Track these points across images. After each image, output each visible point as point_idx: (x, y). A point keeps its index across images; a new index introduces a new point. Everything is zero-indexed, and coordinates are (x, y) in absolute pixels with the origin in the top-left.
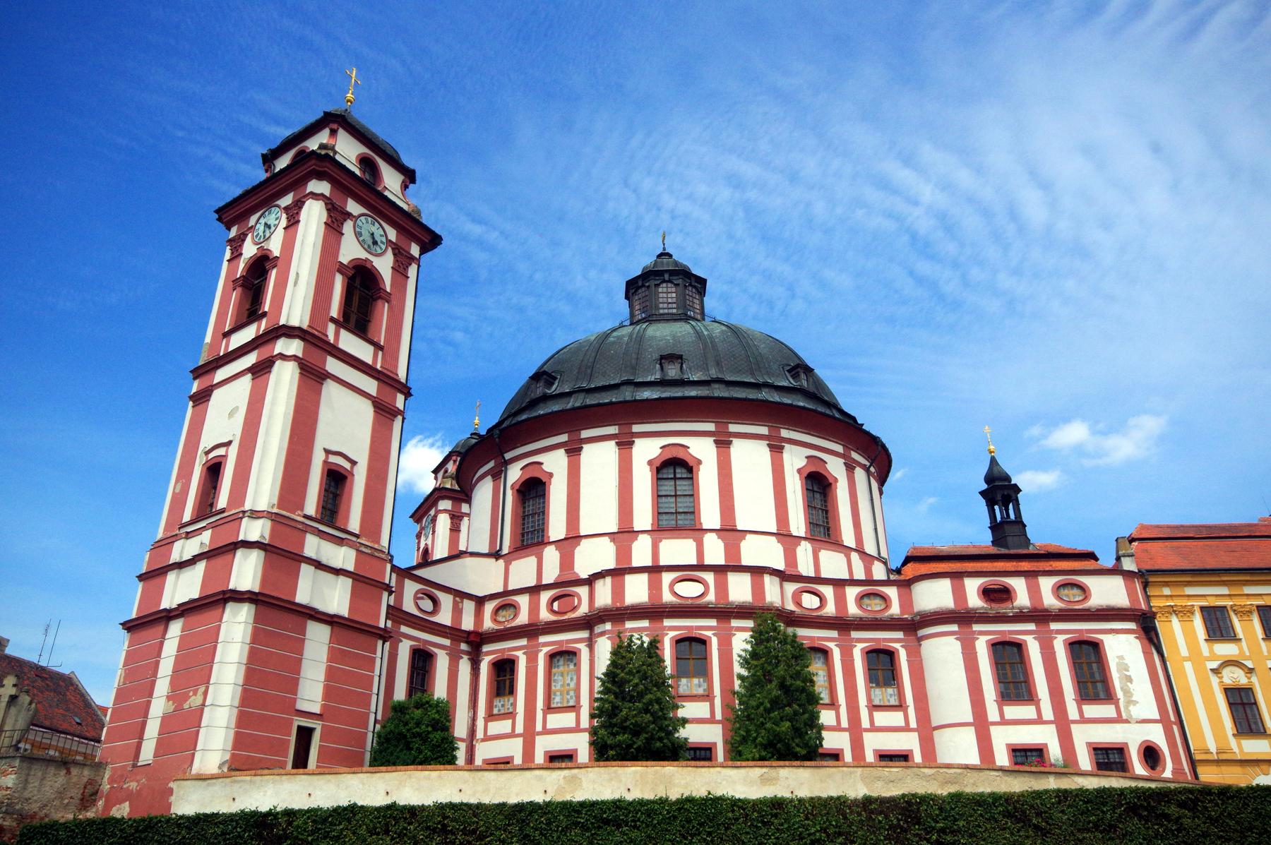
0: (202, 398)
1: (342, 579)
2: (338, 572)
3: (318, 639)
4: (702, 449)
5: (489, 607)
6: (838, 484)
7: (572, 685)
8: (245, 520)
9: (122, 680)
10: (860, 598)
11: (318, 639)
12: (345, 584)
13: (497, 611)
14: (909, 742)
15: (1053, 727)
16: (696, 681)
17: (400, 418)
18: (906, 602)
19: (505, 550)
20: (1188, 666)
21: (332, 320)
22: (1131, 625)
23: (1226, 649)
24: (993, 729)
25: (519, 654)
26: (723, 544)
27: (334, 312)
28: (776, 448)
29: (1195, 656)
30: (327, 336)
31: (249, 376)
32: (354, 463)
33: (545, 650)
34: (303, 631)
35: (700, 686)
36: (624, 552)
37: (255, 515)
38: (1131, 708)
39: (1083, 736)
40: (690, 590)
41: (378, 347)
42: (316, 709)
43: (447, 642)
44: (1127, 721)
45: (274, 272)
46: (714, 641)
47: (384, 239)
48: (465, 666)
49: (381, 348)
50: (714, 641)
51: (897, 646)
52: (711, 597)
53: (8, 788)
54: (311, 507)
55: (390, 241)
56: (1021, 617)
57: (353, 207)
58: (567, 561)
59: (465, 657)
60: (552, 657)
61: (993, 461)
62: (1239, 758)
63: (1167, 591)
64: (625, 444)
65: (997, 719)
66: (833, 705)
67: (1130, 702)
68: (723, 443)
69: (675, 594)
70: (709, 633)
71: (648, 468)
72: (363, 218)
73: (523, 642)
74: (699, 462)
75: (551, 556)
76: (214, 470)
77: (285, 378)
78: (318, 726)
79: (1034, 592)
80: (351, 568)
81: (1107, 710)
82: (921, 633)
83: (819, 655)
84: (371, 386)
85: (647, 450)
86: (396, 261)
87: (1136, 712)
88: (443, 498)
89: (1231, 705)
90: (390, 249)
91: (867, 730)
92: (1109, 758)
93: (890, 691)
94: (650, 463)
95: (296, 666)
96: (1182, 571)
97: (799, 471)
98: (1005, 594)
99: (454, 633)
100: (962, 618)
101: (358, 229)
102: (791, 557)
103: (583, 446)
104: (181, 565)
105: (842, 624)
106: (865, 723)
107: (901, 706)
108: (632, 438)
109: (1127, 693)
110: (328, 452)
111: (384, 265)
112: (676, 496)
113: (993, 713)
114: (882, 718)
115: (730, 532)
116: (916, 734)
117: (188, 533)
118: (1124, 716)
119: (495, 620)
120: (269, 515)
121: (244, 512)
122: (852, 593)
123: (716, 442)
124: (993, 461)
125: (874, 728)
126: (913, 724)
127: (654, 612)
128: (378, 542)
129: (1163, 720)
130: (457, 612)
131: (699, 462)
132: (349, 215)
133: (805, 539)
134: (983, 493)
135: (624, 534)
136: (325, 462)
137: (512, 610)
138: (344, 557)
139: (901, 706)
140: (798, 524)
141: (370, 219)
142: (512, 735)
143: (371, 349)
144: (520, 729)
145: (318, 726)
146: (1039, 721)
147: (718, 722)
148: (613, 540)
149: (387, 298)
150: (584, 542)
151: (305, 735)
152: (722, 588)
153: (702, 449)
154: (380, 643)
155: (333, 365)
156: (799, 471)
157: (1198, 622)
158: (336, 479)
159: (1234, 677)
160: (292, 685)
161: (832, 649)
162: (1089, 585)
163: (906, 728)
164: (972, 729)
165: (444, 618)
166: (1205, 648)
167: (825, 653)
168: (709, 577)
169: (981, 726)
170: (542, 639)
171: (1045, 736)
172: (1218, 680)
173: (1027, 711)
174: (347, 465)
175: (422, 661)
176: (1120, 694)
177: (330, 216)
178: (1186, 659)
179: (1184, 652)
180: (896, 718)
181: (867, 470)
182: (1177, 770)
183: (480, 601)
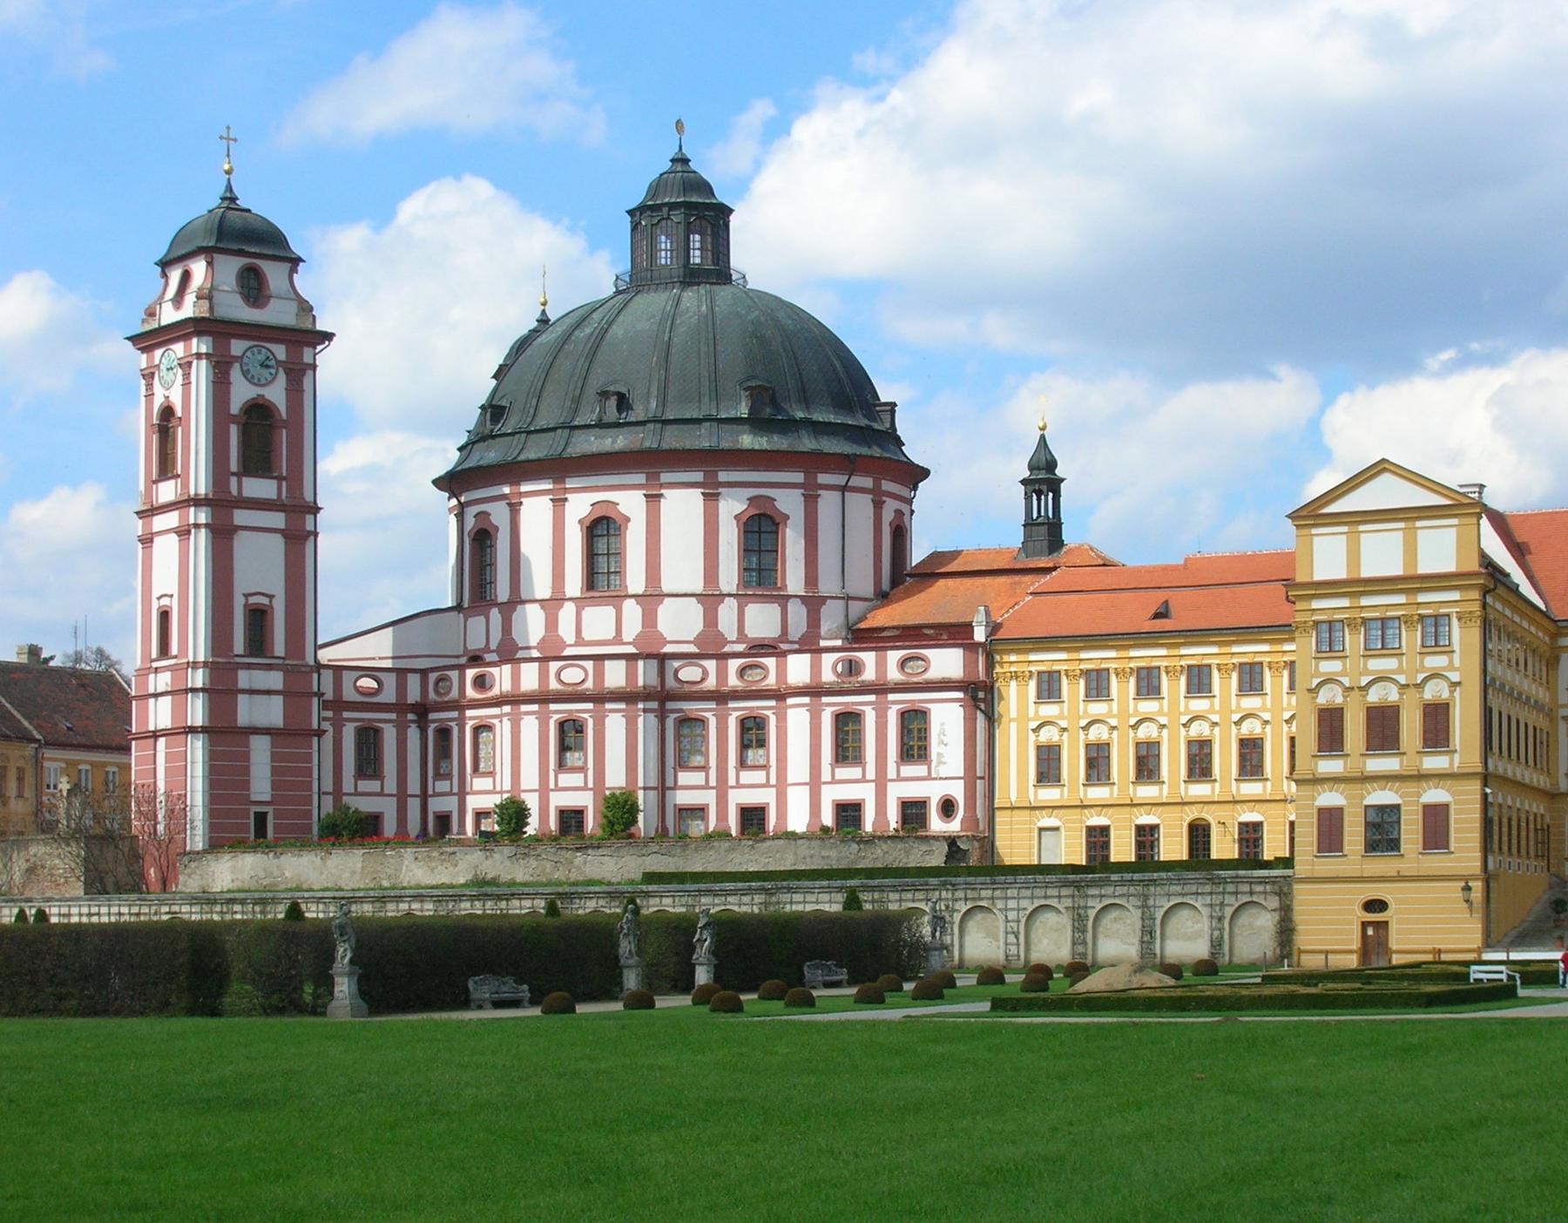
0: (147, 540)
1: (274, 697)
2: (268, 692)
3: (260, 749)
4: (630, 503)
5: (433, 677)
6: (788, 522)
8: (190, 670)
10: (742, 672)
11: (260, 749)
12: (277, 703)
13: (439, 680)
14: (766, 797)
15: (873, 784)
16: (577, 755)
17: (312, 538)
18: (782, 672)
19: (466, 605)
20: (1013, 726)
21: (234, 474)
22: (960, 695)
23: (1049, 710)
24: (824, 787)
25: (453, 724)
26: (640, 610)
27: (234, 467)
28: (711, 498)
29: (1023, 718)
30: (230, 492)
31: (174, 538)
32: (271, 597)
34: (247, 745)
35: (580, 759)
38: (941, 768)
39: (897, 792)
40: (572, 675)
41: (280, 479)
42: (267, 798)
43: (393, 716)
44: (935, 779)
45: (180, 429)
46: (590, 722)
47: (273, 363)
48: (413, 734)
49: (284, 478)
50: (590, 722)
51: (768, 713)
52: (589, 684)
54: (239, 646)
55: (280, 362)
56: (865, 689)
57: (237, 347)
59: (413, 726)
61: (1043, 438)
62: (1033, 805)
63: (1013, 658)
64: (559, 503)
65: (829, 779)
66: (704, 768)
67: (940, 763)
69: (560, 681)
70: (585, 716)
71: (579, 527)
72: (248, 354)
73: (455, 714)
74: (628, 520)
75: (495, 614)
76: (165, 616)
77: (201, 539)
78: (269, 809)
79: (881, 666)
80: (279, 686)
81: (920, 770)
82: (790, 701)
83: (699, 723)
84: (277, 520)
85: (580, 505)
86: (288, 381)
87: (943, 772)
89: (1039, 760)
90: (281, 370)
91: (732, 787)
92: (913, 812)
93: (761, 752)
94: (580, 521)
95: (246, 771)
97: (736, 517)
98: (853, 668)
99: (400, 707)
100: (815, 691)
101: (245, 368)
102: (711, 619)
103: (522, 500)
104: (156, 695)
105: (721, 697)
106: (732, 781)
107: (765, 767)
108: (565, 493)
109: (940, 755)
110: (247, 596)
111: (276, 394)
113: (826, 775)
114: (747, 777)
115: (652, 598)
116: (774, 790)
117: (156, 668)
118: (934, 775)
119: (437, 692)
120: (205, 664)
122: (734, 665)
125: (739, 786)
126: (773, 781)
127: (543, 698)
128: (304, 659)
129: (970, 778)
130: (401, 688)
131: (628, 520)
132: (236, 359)
133: (730, 595)
134: (1024, 482)
135: (553, 604)
136: (246, 605)
137: (448, 683)
138: (275, 680)
139: (765, 767)
140: (729, 577)
141: (255, 349)
142: (450, 794)
143: (275, 482)
144: (455, 790)
145: (269, 809)
146: (863, 780)
147: (591, 789)
148: (542, 608)
149: (285, 424)
151: (261, 819)
152: (599, 675)
153: (630, 503)
154: (315, 739)
155: (241, 517)
156: (736, 517)
157: (1032, 685)
158: (258, 617)
159: (1049, 735)
160: (246, 785)
161: (708, 719)
162: (930, 658)
163: (767, 785)
164: (807, 788)
165: (389, 696)
166: (1032, 706)
167: (702, 722)
168: (589, 665)
169: (815, 784)
170: (469, 713)
171: (864, 793)
172: (1035, 738)
173: (855, 772)
174: (265, 601)
175: (369, 740)
176: (934, 756)
177: (215, 374)
178: (1014, 720)
179: (1013, 714)
180: (759, 777)
181: (844, 489)
182: (970, 820)
183: (424, 673)
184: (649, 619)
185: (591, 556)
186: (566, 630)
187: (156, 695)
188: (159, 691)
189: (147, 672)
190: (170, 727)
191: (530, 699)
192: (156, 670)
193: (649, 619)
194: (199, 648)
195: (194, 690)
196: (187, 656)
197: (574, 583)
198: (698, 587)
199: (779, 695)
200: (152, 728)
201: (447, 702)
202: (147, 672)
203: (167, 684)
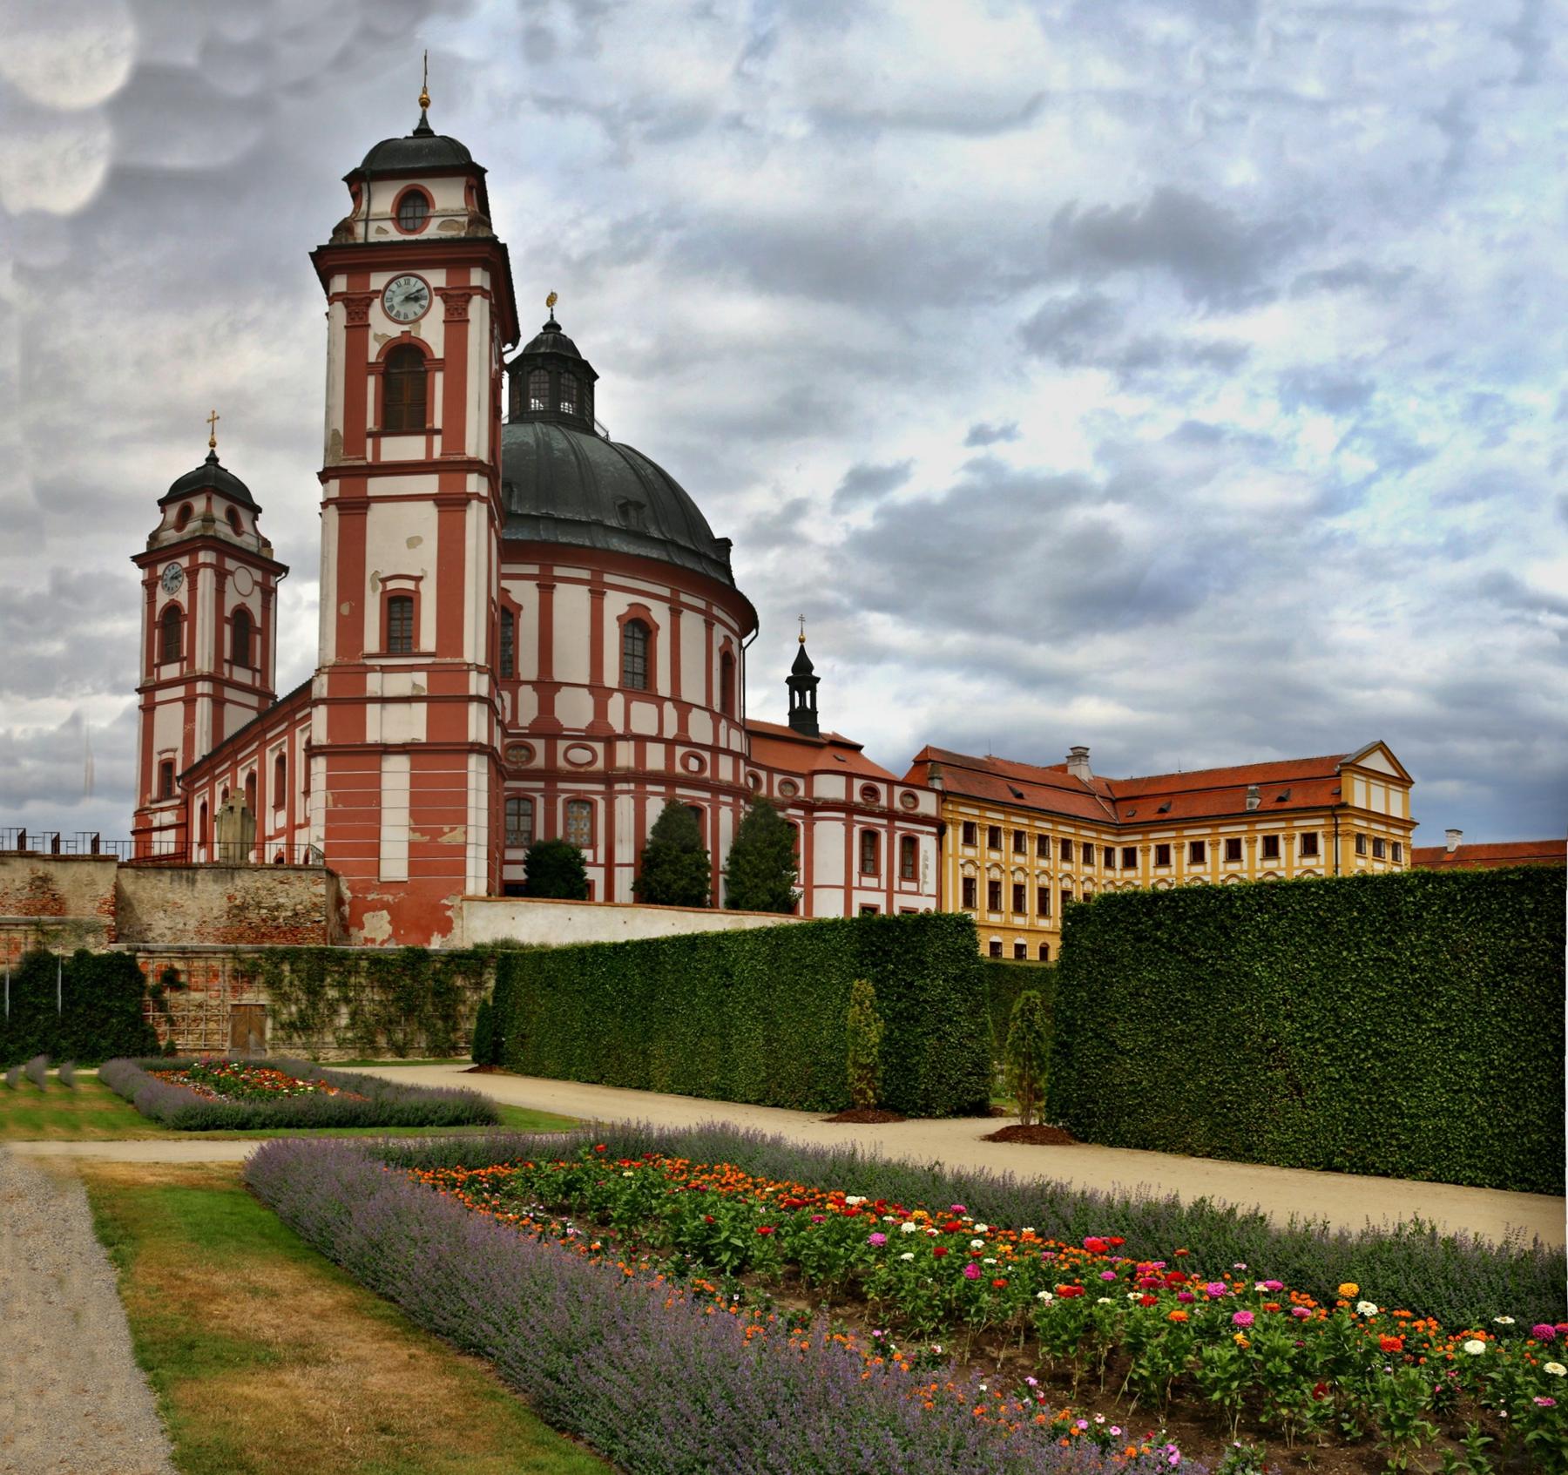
7: (586, 830)
9: (330, 802)
25: (537, 795)
28: (709, 626)
33: (564, 796)
36: (601, 710)
37: (480, 669)
46: (709, 810)
50: (709, 810)
53: (322, 896)
58: (546, 706)
60: (568, 802)
61: (802, 650)
68: (675, 613)
71: (616, 624)
73: (541, 785)
76: (400, 605)
88: (206, 548)
96: (1069, 816)
104: (384, 700)
112: (634, 656)
117: (381, 666)
121: (469, 665)
123: (670, 609)
124: (802, 650)
127: (666, 779)
137: (524, 752)
150: (564, 689)
170: (561, 785)
184: (683, 724)
185: (624, 654)
186: (616, 722)
187: (384, 700)
188: (388, 694)
189: (362, 670)
190: (424, 740)
191: (656, 778)
192: (384, 669)
193: (683, 724)
194: (474, 647)
195: (479, 699)
196: (460, 653)
197: (611, 677)
198: (703, 703)
199: (812, 807)
200: (372, 737)
201: (527, 771)
202: (362, 670)
203: (415, 686)
